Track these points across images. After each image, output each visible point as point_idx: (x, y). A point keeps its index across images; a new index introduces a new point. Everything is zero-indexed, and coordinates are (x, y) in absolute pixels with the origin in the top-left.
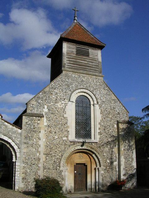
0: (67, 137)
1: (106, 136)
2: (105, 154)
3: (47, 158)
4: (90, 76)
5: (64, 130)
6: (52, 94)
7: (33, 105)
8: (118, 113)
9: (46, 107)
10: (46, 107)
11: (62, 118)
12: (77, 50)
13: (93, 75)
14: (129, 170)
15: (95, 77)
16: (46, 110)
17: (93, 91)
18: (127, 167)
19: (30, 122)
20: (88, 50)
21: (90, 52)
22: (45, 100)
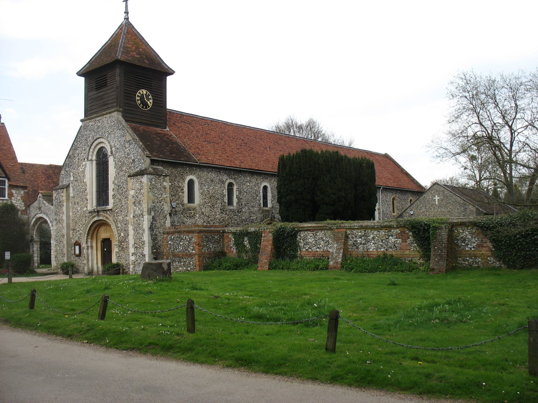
0: (87, 207)
1: (120, 199)
2: (119, 225)
3: (74, 233)
4: (105, 116)
5: (84, 199)
6: (75, 156)
7: (63, 175)
8: (133, 160)
9: (72, 174)
10: (72, 174)
11: (83, 184)
12: (96, 84)
13: (107, 114)
14: (139, 247)
15: (108, 115)
16: (72, 179)
17: (107, 138)
18: (136, 243)
19: (57, 196)
20: (106, 75)
21: (109, 78)
22: (71, 166)
